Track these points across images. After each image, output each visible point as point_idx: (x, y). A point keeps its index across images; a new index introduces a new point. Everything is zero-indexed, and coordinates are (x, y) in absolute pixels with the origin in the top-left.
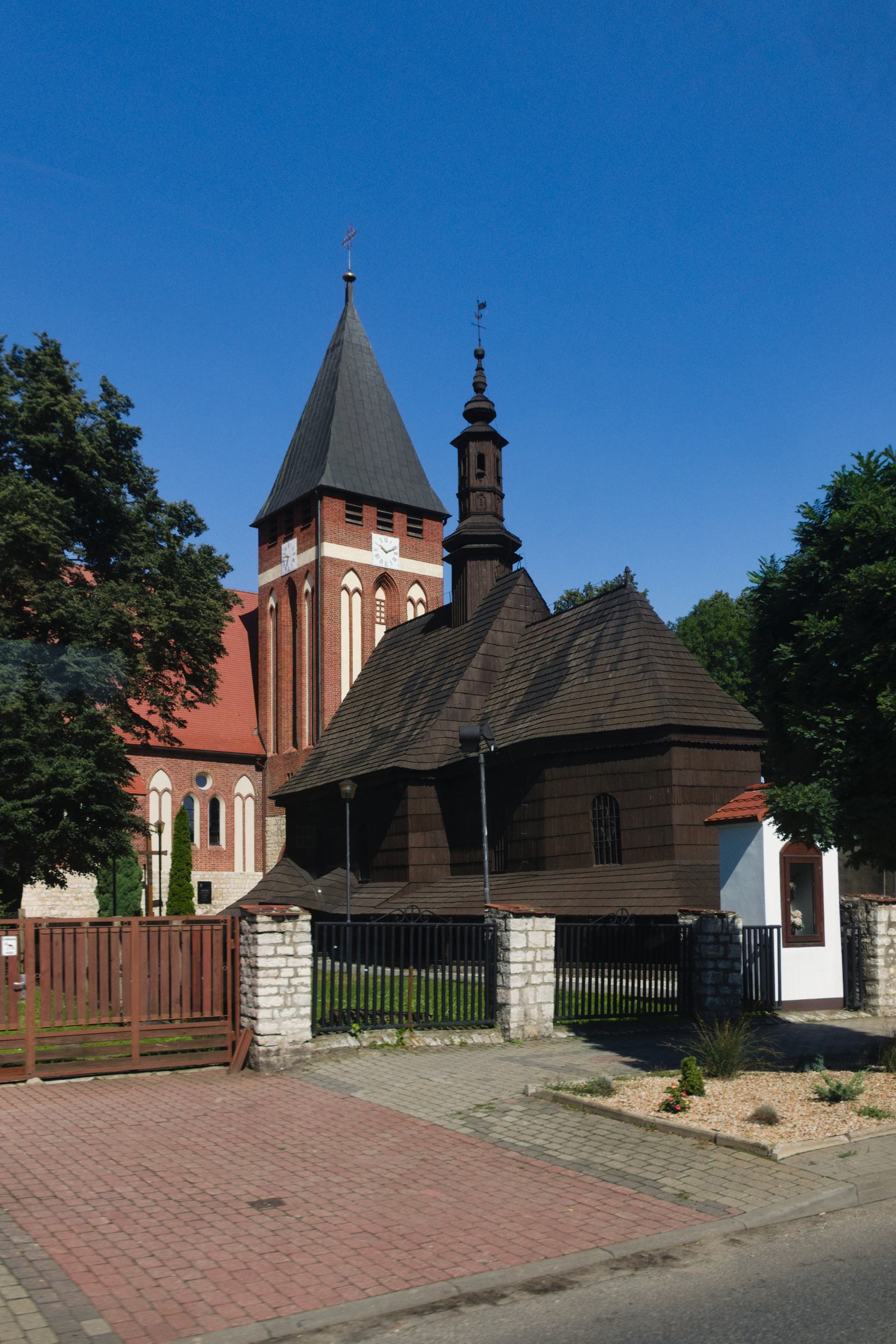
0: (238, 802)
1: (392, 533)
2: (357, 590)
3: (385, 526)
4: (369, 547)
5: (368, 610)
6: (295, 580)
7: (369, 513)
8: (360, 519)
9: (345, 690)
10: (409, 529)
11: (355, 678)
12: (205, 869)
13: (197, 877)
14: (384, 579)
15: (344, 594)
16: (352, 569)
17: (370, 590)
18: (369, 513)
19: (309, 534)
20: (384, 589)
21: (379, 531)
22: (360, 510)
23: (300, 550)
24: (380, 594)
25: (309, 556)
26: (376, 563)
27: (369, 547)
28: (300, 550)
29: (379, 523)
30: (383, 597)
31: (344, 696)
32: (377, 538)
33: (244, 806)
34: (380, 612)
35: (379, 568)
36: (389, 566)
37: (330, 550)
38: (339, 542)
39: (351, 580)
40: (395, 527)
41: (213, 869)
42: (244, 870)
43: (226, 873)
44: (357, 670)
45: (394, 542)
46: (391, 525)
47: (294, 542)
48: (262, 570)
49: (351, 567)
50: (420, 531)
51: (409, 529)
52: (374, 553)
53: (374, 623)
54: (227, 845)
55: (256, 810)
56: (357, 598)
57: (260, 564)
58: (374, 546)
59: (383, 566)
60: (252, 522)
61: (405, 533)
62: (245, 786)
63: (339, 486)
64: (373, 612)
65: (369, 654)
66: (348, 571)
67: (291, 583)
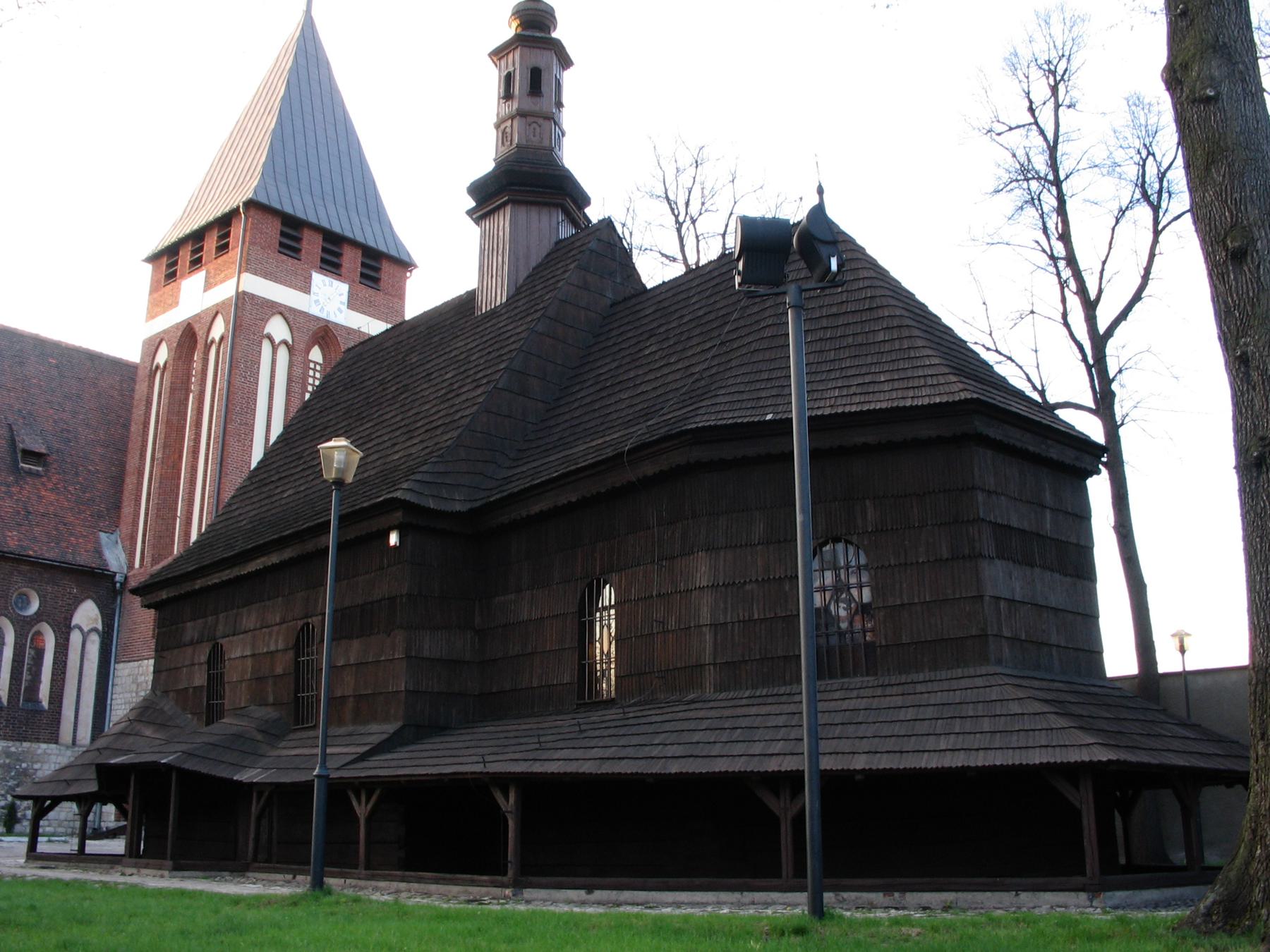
0: (76, 637)
2: (285, 342)
3: (331, 266)
4: (306, 289)
5: (298, 371)
6: (197, 327)
7: (312, 245)
9: (257, 455)
11: (273, 439)
15: (266, 348)
16: (281, 314)
17: (302, 346)
18: (312, 245)
20: (322, 349)
23: (208, 286)
24: (316, 355)
26: (315, 311)
27: (306, 289)
28: (208, 286)
30: (319, 359)
31: (254, 465)
32: (318, 279)
34: (314, 377)
35: (318, 319)
36: (332, 318)
38: (267, 275)
39: (277, 328)
40: (344, 270)
41: (25, 739)
43: (44, 746)
44: (277, 429)
45: (342, 288)
47: (199, 277)
48: (151, 316)
54: (50, 703)
56: (283, 354)
57: (149, 312)
58: (314, 289)
59: (323, 315)
60: (145, 255)
61: (358, 278)
62: (87, 614)
64: (305, 377)
65: (296, 405)
66: (273, 314)
67: (188, 339)
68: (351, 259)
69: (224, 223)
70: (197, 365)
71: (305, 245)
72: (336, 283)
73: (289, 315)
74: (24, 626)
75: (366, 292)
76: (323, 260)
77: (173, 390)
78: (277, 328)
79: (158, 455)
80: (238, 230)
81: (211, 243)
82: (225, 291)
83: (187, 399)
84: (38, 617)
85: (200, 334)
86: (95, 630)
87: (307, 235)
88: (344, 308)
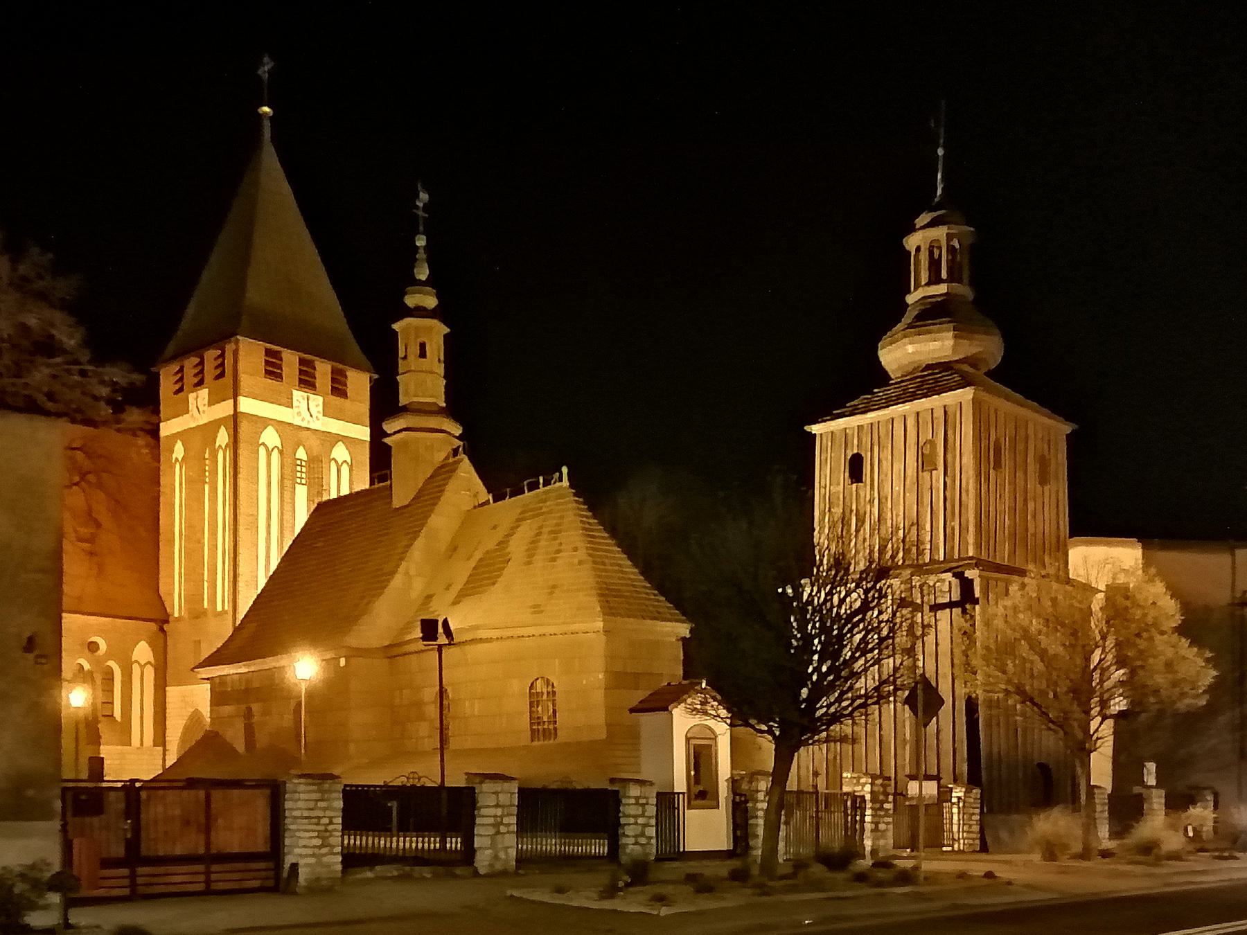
0: (136, 670)
4: (290, 405)
15: (262, 450)
25: (225, 409)
27: (290, 405)
32: (298, 395)
37: (247, 405)
39: (270, 437)
42: (142, 744)
45: (317, 401)
47: (204, 393)
49: (265, 422)
52: (296, 410)
55: (155, 679)
56: (275, 456)
58: (295, 403)
73: (280, 426)
75: (337, 400)
76: (301, 381)
82: (225, 409)
84: (109, 655)
86: (149, 663)
88: (321, 416)
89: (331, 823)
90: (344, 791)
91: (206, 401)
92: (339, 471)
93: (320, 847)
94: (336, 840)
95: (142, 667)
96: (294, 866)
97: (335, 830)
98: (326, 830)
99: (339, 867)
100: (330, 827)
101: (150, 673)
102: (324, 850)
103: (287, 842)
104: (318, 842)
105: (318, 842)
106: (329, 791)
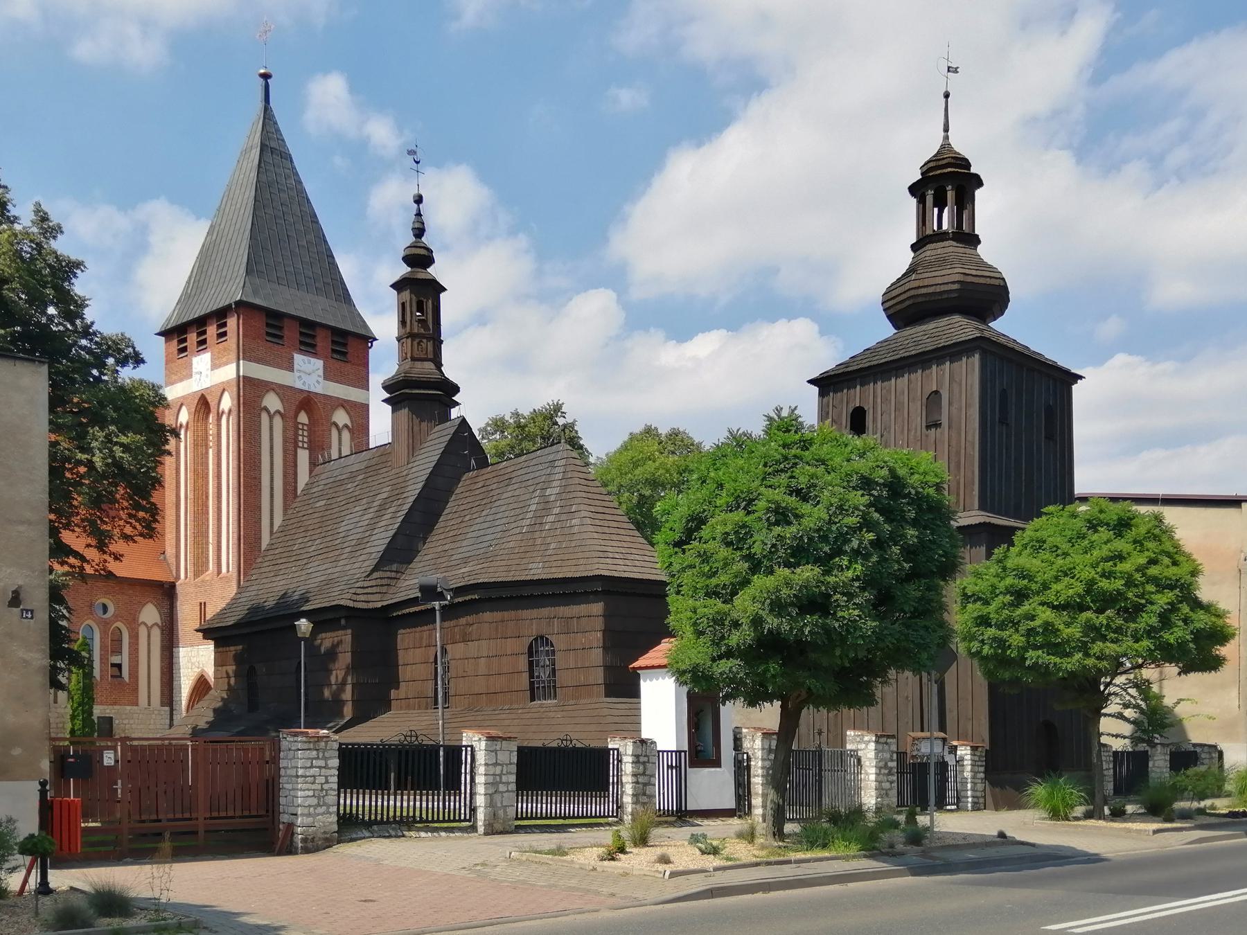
0: (143, 632)
1: (315, 355)
2: (278, 412)
3: (309, 347)
4: (290, 367)
5: (290, 434)
6: (209, 399)
7: (291, 333)
8: (281, 337)
10: (334, 351)
12: (106, 704)
13: (98, 711)
14: (307, 402)
15: (265, 417)
17: (292, 414)
18: (291, 333)
19: (225, 350)
20: (307, 413)
21: (301, 352)
22: (281, 328)
23: (215, 366)
24: (303, 418)
26: (299, 385)
27: (290, 367)
28: (215, 366)
29: (301, 343)
30: (306, 422)
32: (299, 359)
33: (149, 636)
35: (302, 391)
36: (312, 389)
39: (272, 402)
41: (115, 704)
45: (317, 364)
46: (313, 346)
50: (344, 354)
51: (334, 351)
52: (297, 374)
53: (296, 446)
56: (278, 421)
63: (258, 301)
64: (296, 435)
68: (323, 341)
69: (220, 315)
70: (212, 430)
71: (286, 333)
72: (313, 360)
74: (105, 625)
75: (338, 364)
77: (196, 445)
78: (272, 402)
79: (190, 495)
80: (232, 322)
81: (212, 330)
82: (228, 372)
83: (207, 453)
84: (116, 617)
85: (213, 404)
86: (156, 624)
87: (286, 323)
88: (321, 380)
89: (327, 782)
90: (340, 749)
91: (209, 366)
92: (340, 434)
93: (316, 807)
94: (332, 799)
95: (149, 629)
96: (290, 826)
97: (331, 789)
98: (322, 789)
99: (335, 827)
100: (326, 787)
101: (156, 635)
102: (320, 810)
103: (282, 801)
104: (314, 801)
105: (314, 801)
106: (324, 750)
